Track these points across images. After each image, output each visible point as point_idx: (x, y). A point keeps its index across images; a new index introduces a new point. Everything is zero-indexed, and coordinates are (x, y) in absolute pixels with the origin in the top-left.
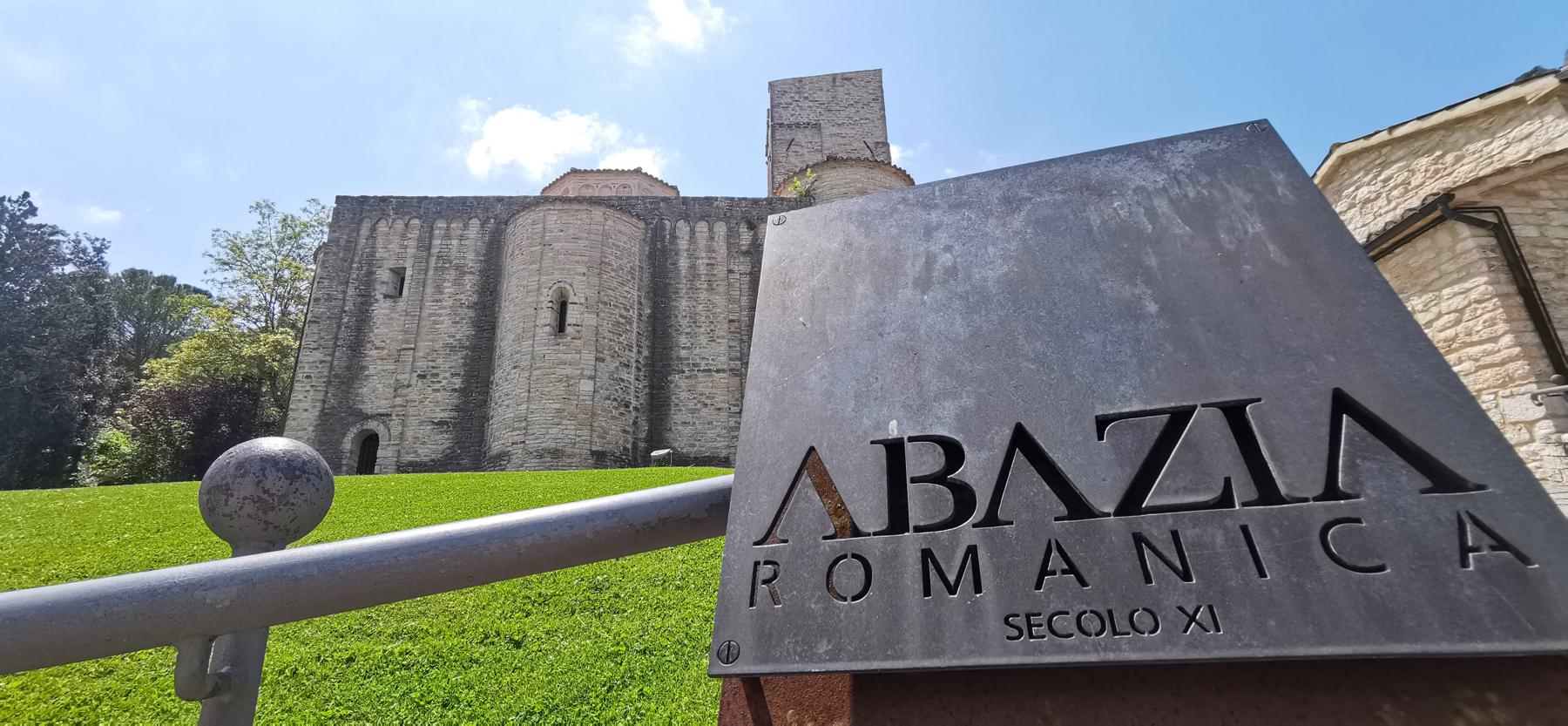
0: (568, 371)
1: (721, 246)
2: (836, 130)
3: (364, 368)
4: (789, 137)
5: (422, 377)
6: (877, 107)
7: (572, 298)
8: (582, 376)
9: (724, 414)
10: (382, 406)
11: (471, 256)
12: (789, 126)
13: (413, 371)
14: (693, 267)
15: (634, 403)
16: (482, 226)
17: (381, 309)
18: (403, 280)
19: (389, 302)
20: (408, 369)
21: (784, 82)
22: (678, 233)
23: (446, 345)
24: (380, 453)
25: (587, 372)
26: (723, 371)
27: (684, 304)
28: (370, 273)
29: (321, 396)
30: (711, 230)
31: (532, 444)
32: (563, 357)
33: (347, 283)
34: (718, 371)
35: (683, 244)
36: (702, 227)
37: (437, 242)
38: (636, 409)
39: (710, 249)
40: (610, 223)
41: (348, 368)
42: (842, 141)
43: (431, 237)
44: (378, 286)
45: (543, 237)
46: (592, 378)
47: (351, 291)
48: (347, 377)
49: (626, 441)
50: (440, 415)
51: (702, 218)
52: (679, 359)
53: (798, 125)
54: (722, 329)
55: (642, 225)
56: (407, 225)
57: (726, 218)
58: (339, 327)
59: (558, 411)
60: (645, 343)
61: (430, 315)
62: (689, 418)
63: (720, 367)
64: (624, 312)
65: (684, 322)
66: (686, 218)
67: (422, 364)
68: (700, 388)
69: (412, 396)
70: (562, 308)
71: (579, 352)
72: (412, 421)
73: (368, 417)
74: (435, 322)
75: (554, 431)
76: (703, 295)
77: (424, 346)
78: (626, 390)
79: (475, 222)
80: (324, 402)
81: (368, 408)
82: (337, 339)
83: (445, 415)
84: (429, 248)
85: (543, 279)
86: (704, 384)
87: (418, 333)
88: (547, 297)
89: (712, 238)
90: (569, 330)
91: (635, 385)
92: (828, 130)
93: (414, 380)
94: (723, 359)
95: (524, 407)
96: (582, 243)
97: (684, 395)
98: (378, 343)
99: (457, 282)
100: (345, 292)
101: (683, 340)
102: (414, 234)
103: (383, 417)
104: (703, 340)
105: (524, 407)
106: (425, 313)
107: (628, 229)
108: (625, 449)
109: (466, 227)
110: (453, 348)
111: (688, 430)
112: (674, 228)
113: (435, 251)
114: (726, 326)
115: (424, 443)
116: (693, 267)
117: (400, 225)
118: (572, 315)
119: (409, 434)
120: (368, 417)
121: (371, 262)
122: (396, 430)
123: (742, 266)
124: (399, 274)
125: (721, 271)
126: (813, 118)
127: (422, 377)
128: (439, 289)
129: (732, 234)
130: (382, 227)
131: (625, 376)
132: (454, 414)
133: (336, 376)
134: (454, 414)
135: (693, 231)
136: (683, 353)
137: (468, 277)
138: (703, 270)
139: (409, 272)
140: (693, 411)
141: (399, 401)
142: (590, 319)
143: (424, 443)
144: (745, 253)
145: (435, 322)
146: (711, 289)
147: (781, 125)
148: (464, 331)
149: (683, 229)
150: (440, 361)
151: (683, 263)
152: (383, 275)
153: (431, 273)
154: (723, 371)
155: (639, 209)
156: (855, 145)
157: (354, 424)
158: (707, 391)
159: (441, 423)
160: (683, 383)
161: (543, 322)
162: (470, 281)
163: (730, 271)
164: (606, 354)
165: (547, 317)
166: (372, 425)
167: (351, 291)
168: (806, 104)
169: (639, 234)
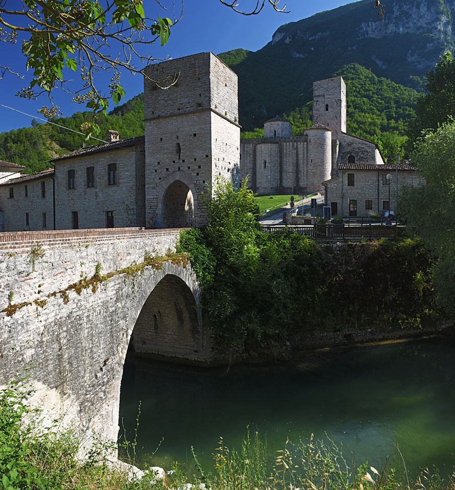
0: (267, 174)
1: (291, 147)
2: (328, 96)
6: (339, 88)
12: (317, 96)
14: (286, 152)
31: (262, 186)
36: (288, 143)
57: (292, 141)
60: (279, 167)
88: (263, 161)
91: (277, 175)
99: (250, 156)
101: (285, 166)
104: (288, 166)
107: (275, 146)
110: (250, 169)
116: (286, 152)
123: (295, 151)
125: (291, 153)
128: (247, 158)
129: (293, 145)
138: (288, 152)
142: (269, 165)
144: (296, 149)
148: (251, 166)
151: (285, 151)
156: (333, 101)
165: (263, 165)
168: (322, 89)
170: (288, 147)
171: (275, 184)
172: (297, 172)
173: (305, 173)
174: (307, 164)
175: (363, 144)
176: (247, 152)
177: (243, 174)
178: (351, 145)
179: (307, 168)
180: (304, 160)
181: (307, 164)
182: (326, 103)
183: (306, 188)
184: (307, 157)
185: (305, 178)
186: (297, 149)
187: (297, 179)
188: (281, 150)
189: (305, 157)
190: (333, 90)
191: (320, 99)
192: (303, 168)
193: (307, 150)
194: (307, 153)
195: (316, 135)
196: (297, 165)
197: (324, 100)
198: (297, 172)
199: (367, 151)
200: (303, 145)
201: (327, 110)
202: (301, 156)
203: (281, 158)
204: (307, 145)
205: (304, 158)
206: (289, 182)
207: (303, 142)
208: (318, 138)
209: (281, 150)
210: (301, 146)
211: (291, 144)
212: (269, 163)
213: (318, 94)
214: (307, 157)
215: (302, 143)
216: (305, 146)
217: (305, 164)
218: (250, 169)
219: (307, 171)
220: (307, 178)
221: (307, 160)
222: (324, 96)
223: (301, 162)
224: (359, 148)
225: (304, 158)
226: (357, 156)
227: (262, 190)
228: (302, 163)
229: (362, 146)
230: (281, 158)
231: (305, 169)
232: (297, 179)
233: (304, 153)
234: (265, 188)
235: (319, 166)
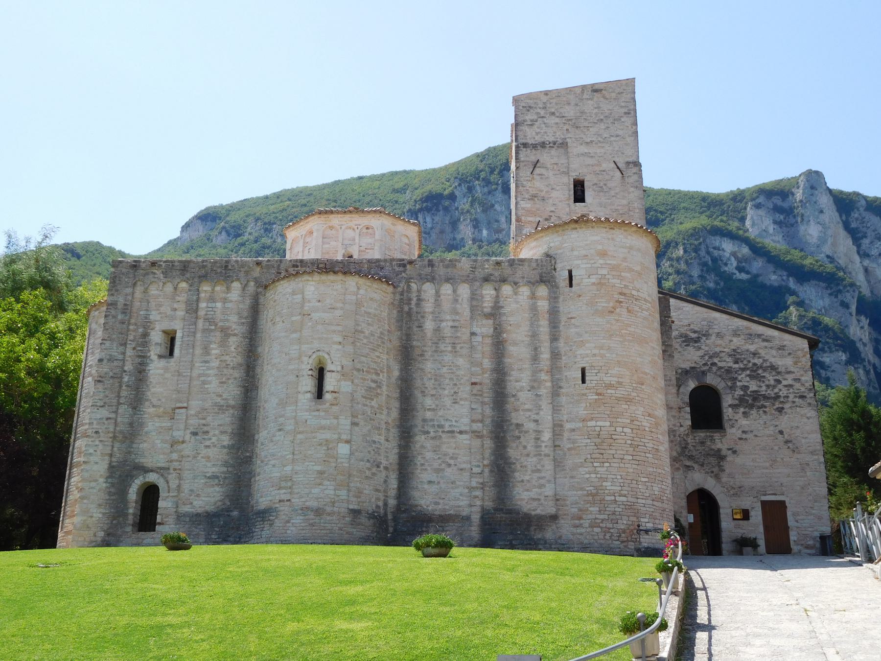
1: (464, 308)
2: (583, 149)
3: (142, 425)
4: (533, 159)
5: (195, 434)
6: (627, 120)
7: (329, 367)
8: (339, 440)
9: (466, 474)
10: (160, 460)
11: (234, 318)
12: (535, 146)
13: (186, 428)
14: (438, 330)
15: (384, 463)
16: (244, 289)
17: (156, 367)
18: (172, 340)
19: (163, 363)
20: (182, 426)
21: (529, 96)
22: (423, 296)
23: (216, 404)
24: (161, 504)
25: (344, 437)
26: (466, 432)
27: (429, 366)
28: (145, 335)
29: (108, 450)
30: (455, 291)
32: (323, 422)
33: (125, 344)
34: (461, 432)
35: (428, 307)
37: (203, 305)
38: (386, 468)
39: (455, 312)
40: (362, 292)
41: (131, 424)
42: (589, 161)
43: (198, 300)
44: (152, 348)
45: (302, 307)
46: (347, 442)
47: (129, 352)
48: (130, 434)
49: (378, 499)
50: (212, 470)
51: (448, 280)
52: (424, 420)
53: (543, 145)
54: (465, 390)
55: (390, 289)
56: (175, 289)
58: (121, 386)
59: (321, 473)
61: (200, 375)
62: (434, 477)
63: (463, 428)
64: (374, 377)
65: (430, 384)
66: (432, 279)
67: (193, 421)
68: (444, 448)
69: (186, 452)
70: (321, 373)
71: (337, 418)
72: (186, 474)
73: (146, 470)
74: (204, 383)
75: (316, 491)
76: (448, 358)
77: (195, 404)
78: (377, 452)
79: (236, 285)
80: (111, 455)
81: (148, 462)
82: (119, 397)
83: (214, 469)
84: (196, 311)
85: (305, 347)
86: (448, 446)
87: (189, 393)
88: (307, 366)
89: (457, 301)
90: (327, 396)
92: (576, 149)
93: (187, 437)
94: (466, 420)
95: (288, 468)
96: (338, 313)
97: (429, 455)
98: (155, 401)
99: (223, 344)
100: (124, 354)
101: (429, 402)
102: (183, 298)
103: (162, 471)
104: (448, 402)
105: (288, 468)
106: (196, 373)
107: (376, 296)
108: (378, 507)
109: (228, 289)
110: (221, 409)
111: (434, 488)
112: (419, 291)
113: (201, 313)
114: (468, 388)
115: (198, 496)
116: (438, 330)
117: (169, 288)
118: (330, 383)
119: (186, 487)
120: (146, 470)
121: (147, 326)
122: (173, 484)
123: (485, 328)
124: (171, 340)
126: (559, 136)
127: (195, 434)
128: (206, 351)
129: (474, 297)
130: (153, 291)
131: (376, 438)
132: (225, 469)
133: (121, 432)
134: (225, 469)
135: (438, 294)
136: (429, 415)
137: (232, 339)
138: (447, 332)
139: (179, 335)
140: (438, 471)
141: (175, 456)
142: (346, 387)
143: (198, 496)
144: (488, 316)
145: (204, 383)
146: (454, 352)
147: (525, 145)
148: (232, 392)
149: (429, 289)
150: (209, 419)
151: (429, 325)
152: (157, 337)
153: (199, 335)
154: (466, 432)
155: (387, 271)
156: (605, 166)
157: (137, 477)
158: (451, 451)
159: (214, 477)
160: (429, 444)
161: (305, 389)
162: (233, 342)
163: (473, 334)
164: (360, 419)
165: (308, 384)
166: (152, 478)
167: (129, 352)
168: (553, 120)
169: (389, 298)
170: (446, 305)
171: (376, 492)
172: (500, 432)
173: (547, 436)
174: (556, 392)
175: (751, 336)
176: (209, 320)
177: (178, 434)
178: (697, 340)
179: (556, 409)
180: (535, 372)
181: (556, 392)
182: (574, 175)
183: (554, 518)
184: (555, 355)
185: (548, 465)
186: (495, 313)
187: (501, 470)
188: (407, 317)
189: (545, 356)
190: (603, 126)
191: (546, 157)
192: (529, 409)
193: (554, 324)
194: (554, 338)
195: (603, 254)
196: (500, 396)
197: (563, 161)
198: (500, 432)
199: (773, 368)
200: (533, 296)
201: (579, 197)
202: (518, 351)
203: (407, 355)
204: (554, 298)
205: (535, 358)
206: (451, 479)
207: (532, 284)
208: (613, 268)
209: (407, 317)
210: (517, 302)
211: (464, 290)
212: (344, 374)
213: (538, 139)
214: (555, 355)
215: (525, 291)
216: (543, 305)
217: (543, 391)
218: (221, 409)
219: (557, 428)
220: (558, 464)
221: (555, 368)
222: (564, 145)
223: (519, 380)
224: (735, 355)
225: (535, 358)
226: (733, 388)
227: (298, 520)
228: (525, 383)
229: (752, 348)
230: (407, 355)
231: (546, 415)
232: (501, 470)
233: (534, 336)
234: (318, 512)
235: (629, 400)
